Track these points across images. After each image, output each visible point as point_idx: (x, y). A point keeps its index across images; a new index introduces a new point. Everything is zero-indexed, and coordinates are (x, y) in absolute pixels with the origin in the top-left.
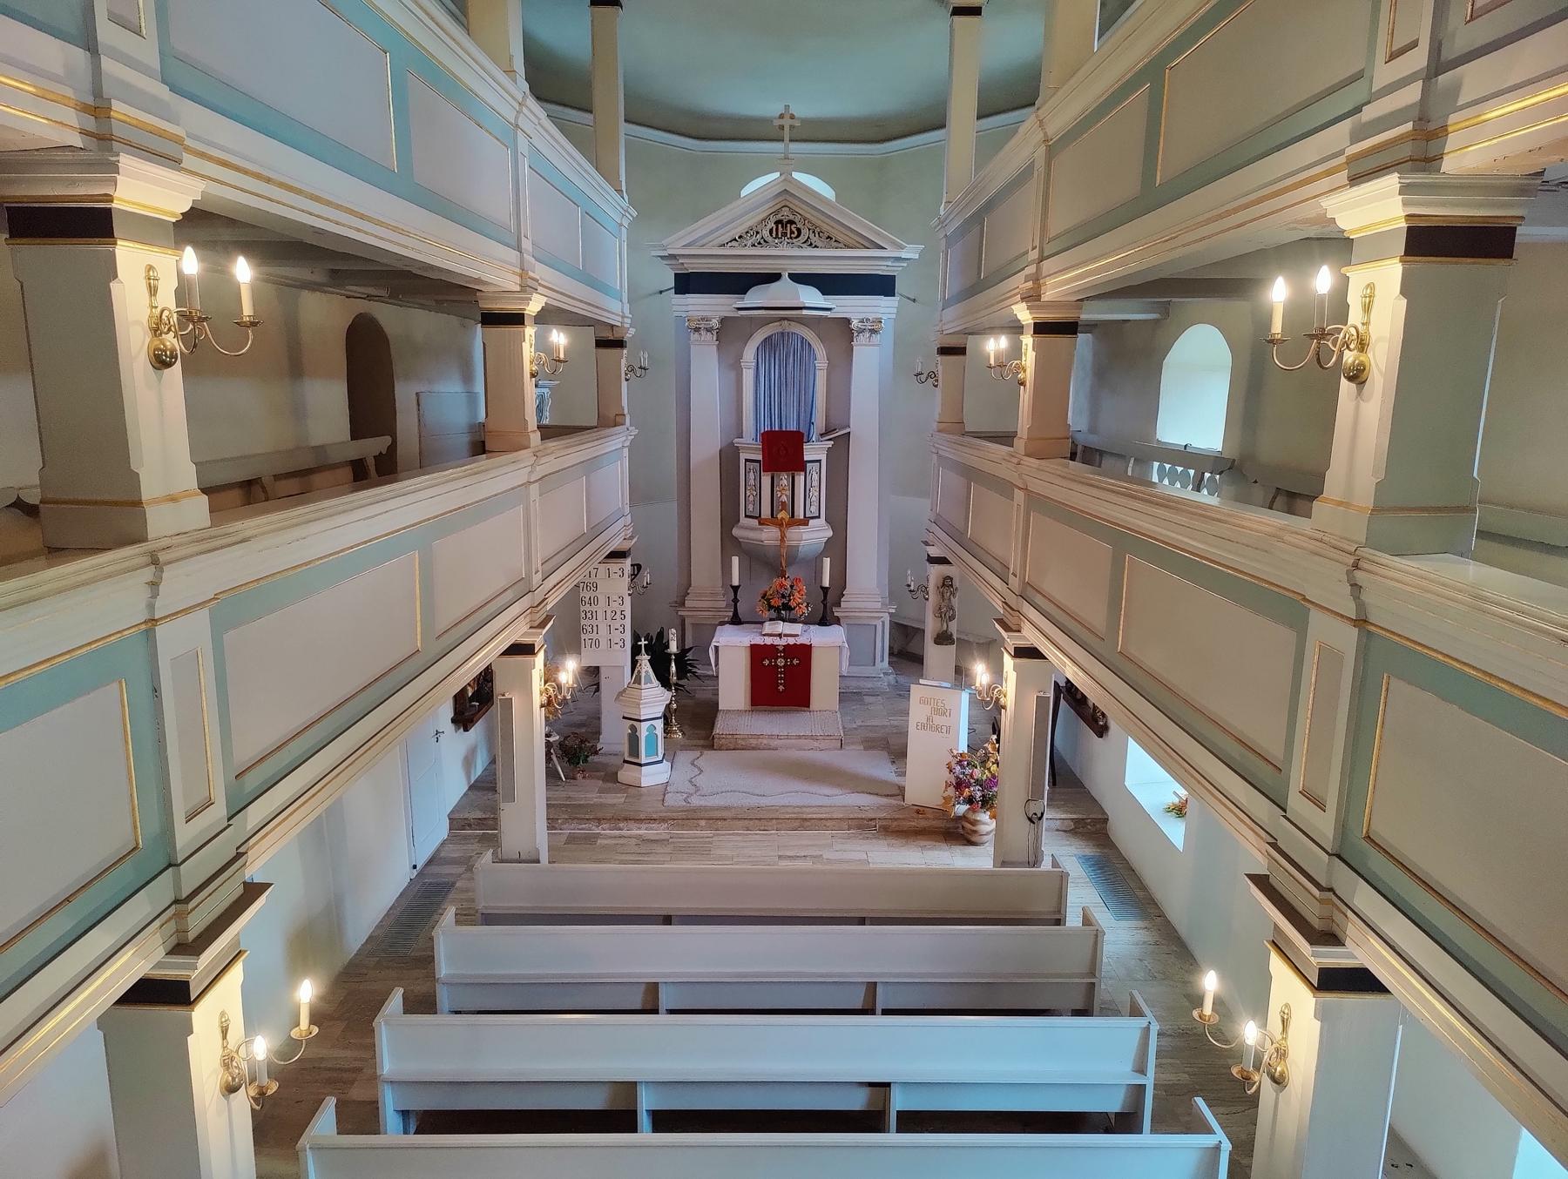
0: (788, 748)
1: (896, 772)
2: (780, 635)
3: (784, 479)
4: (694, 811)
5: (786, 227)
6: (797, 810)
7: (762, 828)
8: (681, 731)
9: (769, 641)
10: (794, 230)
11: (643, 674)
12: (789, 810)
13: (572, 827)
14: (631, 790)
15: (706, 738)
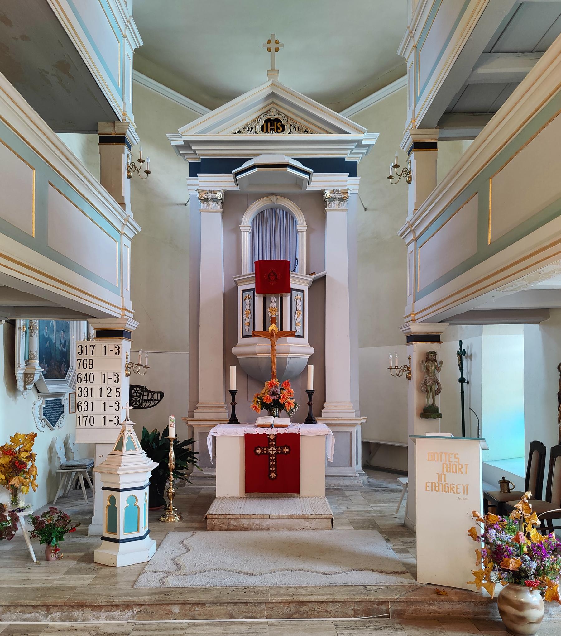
0: (278, 528)
1: (394, 549)
2: (271, 426)
3: (273, 302)
4: (167, 593)
5: (274, 124)
6: (291, 591)
7: (249, 615)
9: (261, 431)
10: (280, 127)
11: (126, 440)
12: (283, 591)
13: (14, 617)
14: (105, 571)
15: (201, 522)
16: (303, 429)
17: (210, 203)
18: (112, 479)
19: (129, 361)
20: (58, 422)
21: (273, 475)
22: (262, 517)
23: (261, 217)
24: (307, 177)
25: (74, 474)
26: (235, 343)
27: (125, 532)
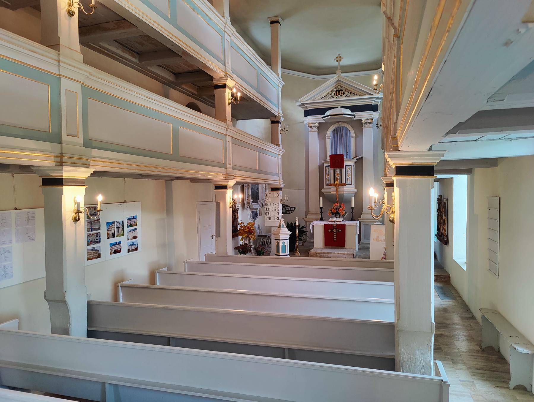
2: (334, 221)
3: (338, 171)
8: (299, 253)
9: (330, 223)
10: (342, 93)
11: (281, 225)
16: (347, 223)
17: (313, 128)
18: (278, 236)
19: (281, 198)
20: (256, 219)
21: (335, 240)
22: (328, 253)
23: (335, 131)
24: (353, 116)
25: (262, 239)
26: (323, 188)
27: (282, 253)
